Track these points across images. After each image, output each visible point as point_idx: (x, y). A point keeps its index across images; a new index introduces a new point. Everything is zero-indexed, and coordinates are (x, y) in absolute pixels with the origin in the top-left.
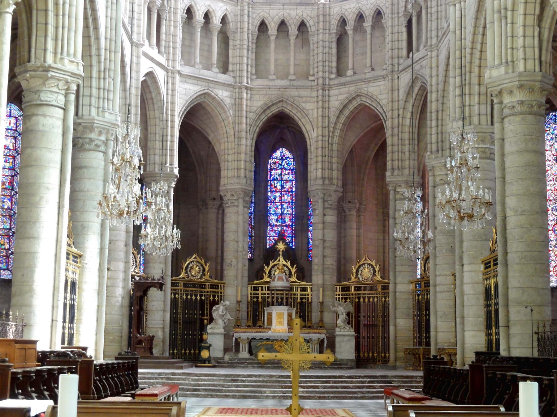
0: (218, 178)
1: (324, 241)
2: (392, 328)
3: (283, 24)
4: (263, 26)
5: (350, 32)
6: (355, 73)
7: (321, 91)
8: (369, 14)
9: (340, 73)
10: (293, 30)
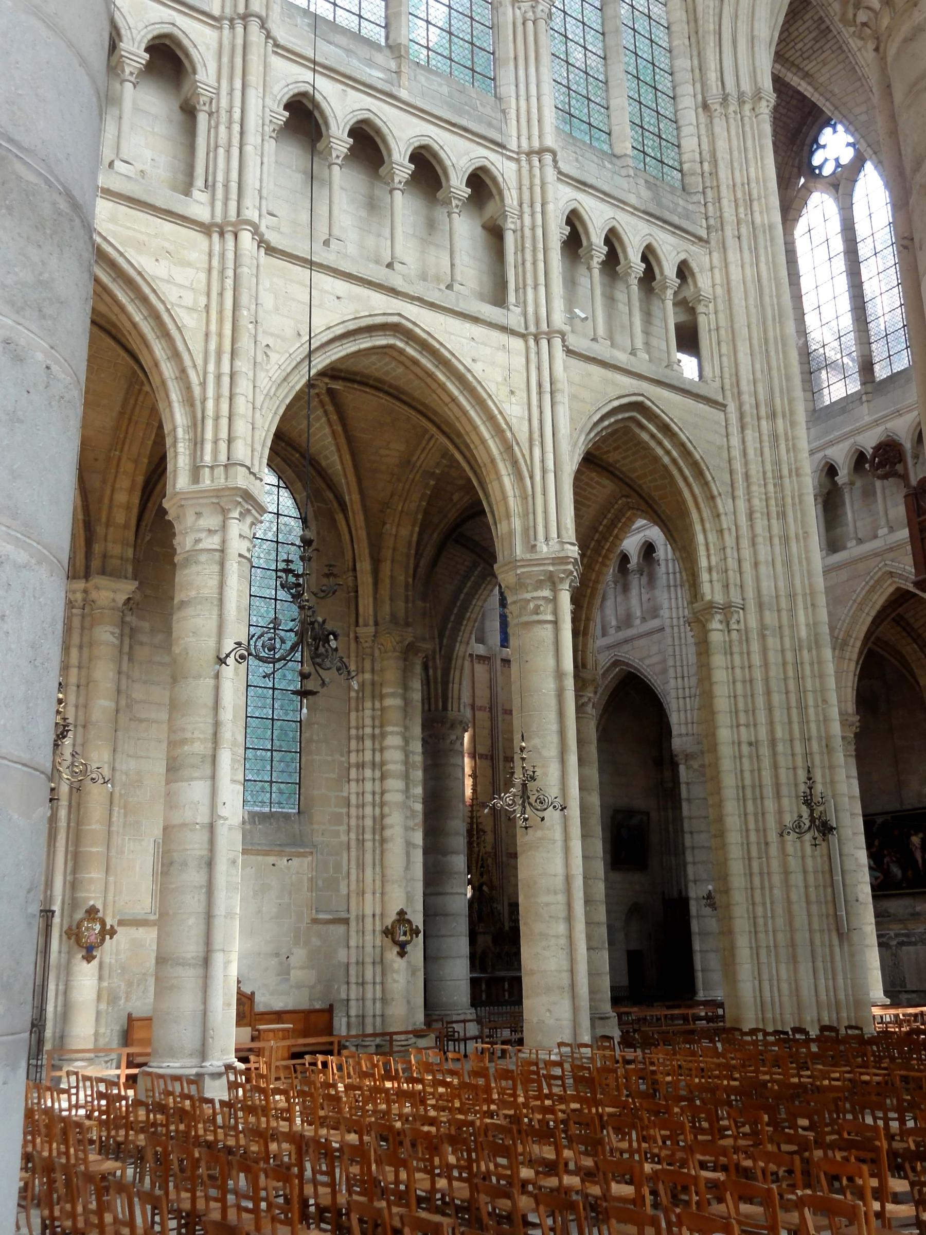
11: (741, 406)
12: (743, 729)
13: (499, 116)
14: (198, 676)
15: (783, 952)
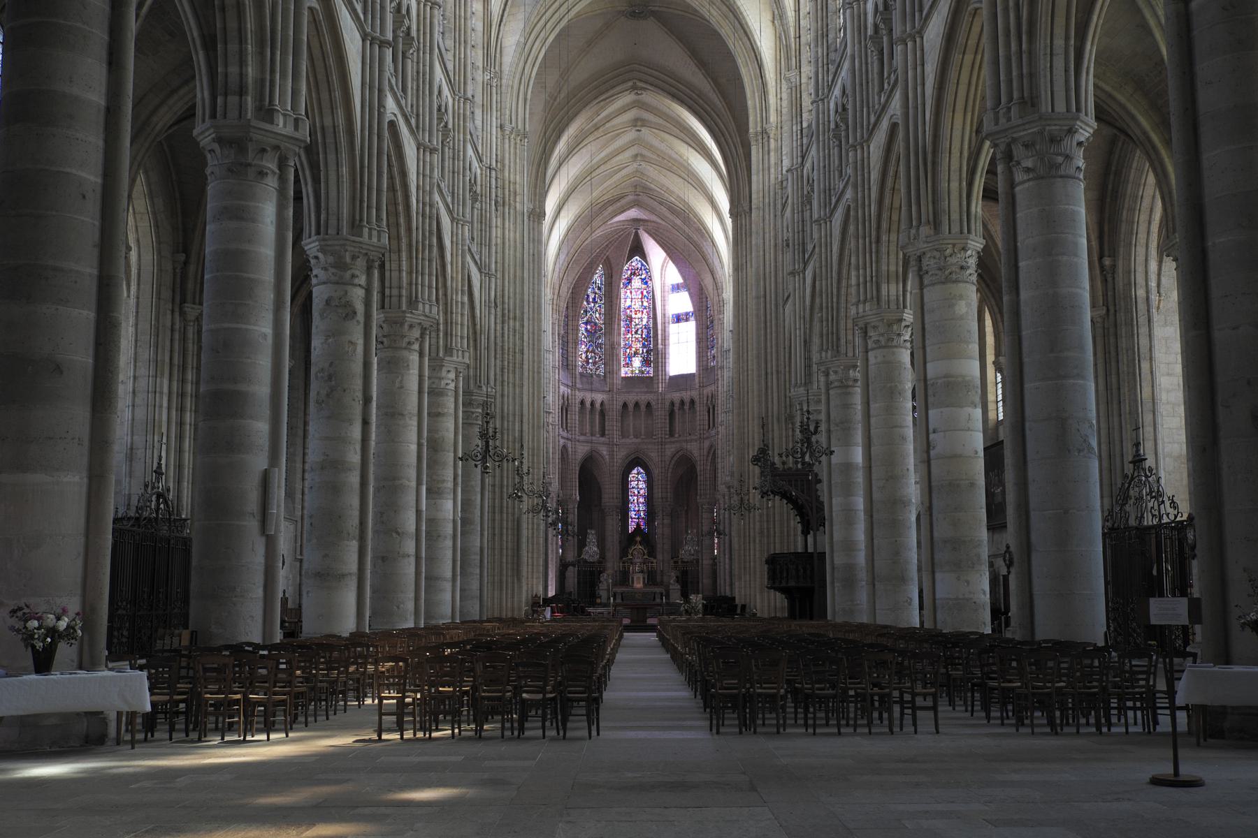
0: (600, 498)
1: (663, 534)
2: (700, 585)
3: (637, 405)
4: (625, 405)
5: (677, 411)
6: (680, 436)
7: (660, 447)
8: (687, 400)
9: (672, 434)
10: (643, 407)
11: (503, 309)
14: (448, 452)
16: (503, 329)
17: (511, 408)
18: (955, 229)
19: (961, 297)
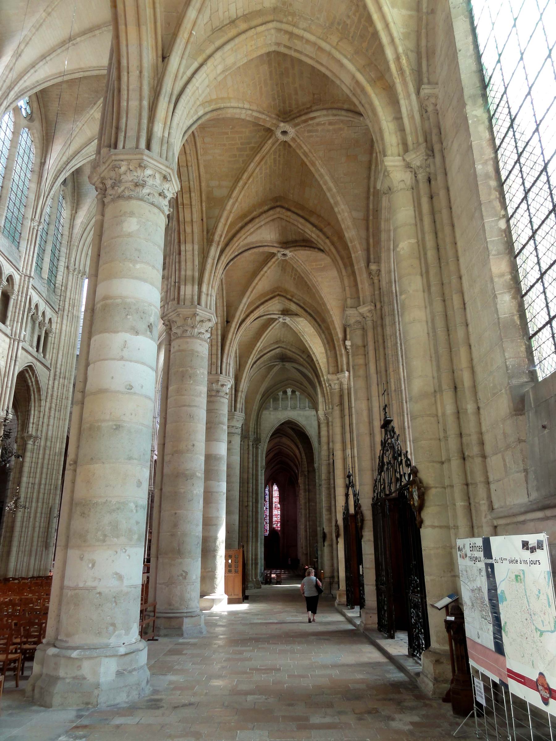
11: (55, 372)
12: (31, 478)
13: (19, 258)
15: (27, 553)
16: (54, 383)
17: (54, 433)
18: (131, 143)
19: (132, 214)
